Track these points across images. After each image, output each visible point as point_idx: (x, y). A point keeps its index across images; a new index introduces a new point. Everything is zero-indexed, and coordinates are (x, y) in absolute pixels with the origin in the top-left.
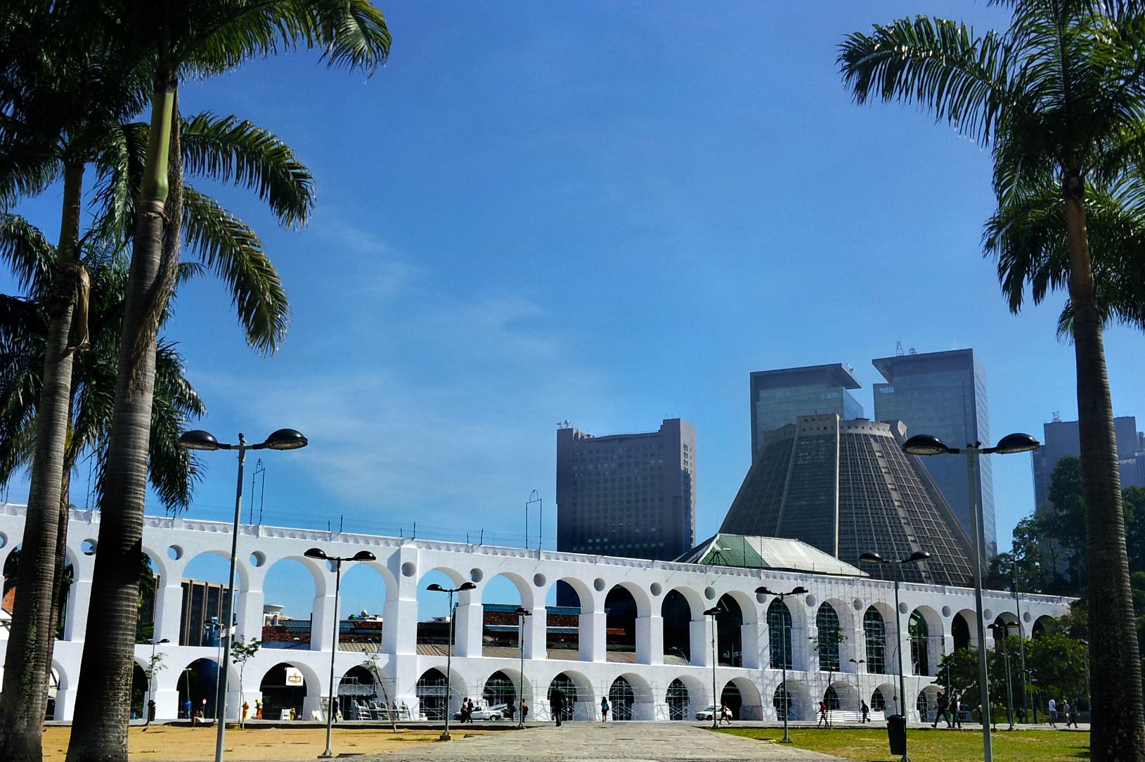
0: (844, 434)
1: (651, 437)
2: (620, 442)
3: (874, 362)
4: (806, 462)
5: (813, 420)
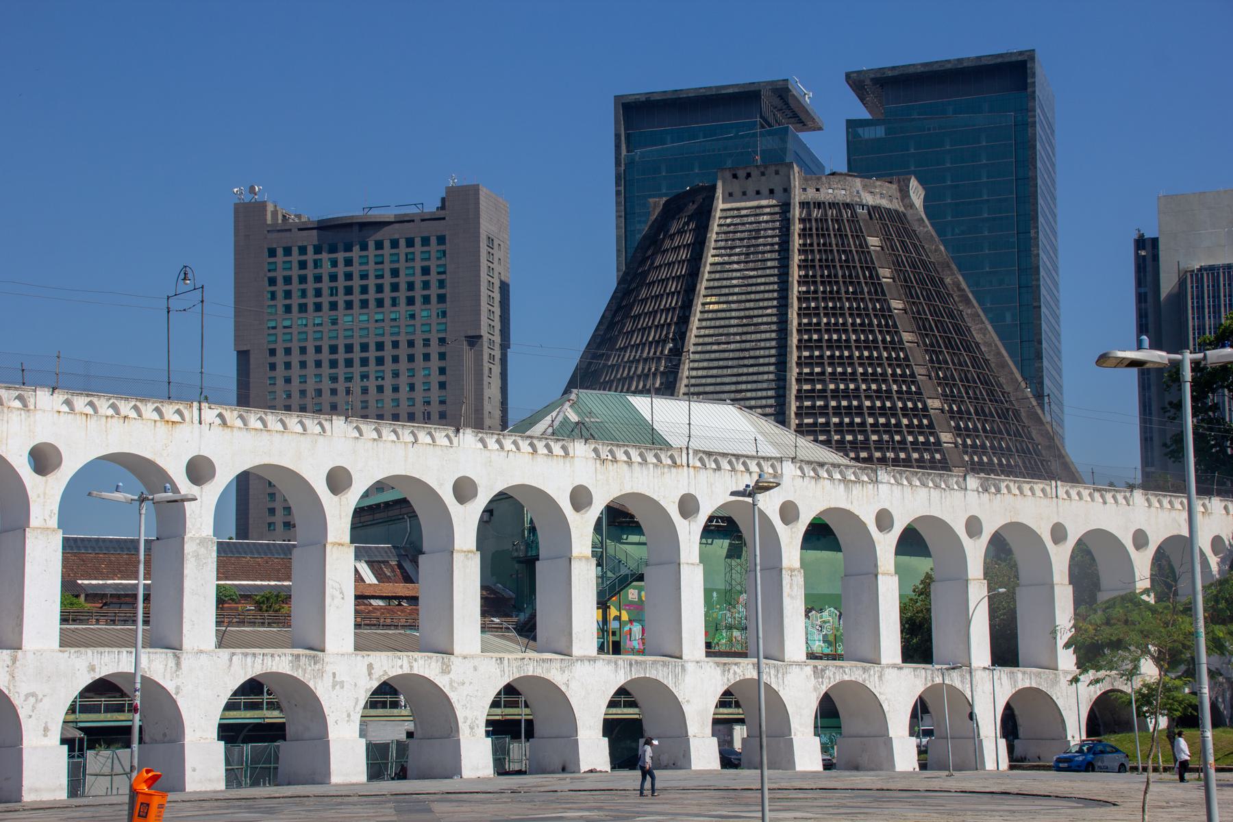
0: (808, 203)
1: (423, 220)
2: (360, 231)
3: (848, 76)
4: (735, 258)
5: (749, 175)
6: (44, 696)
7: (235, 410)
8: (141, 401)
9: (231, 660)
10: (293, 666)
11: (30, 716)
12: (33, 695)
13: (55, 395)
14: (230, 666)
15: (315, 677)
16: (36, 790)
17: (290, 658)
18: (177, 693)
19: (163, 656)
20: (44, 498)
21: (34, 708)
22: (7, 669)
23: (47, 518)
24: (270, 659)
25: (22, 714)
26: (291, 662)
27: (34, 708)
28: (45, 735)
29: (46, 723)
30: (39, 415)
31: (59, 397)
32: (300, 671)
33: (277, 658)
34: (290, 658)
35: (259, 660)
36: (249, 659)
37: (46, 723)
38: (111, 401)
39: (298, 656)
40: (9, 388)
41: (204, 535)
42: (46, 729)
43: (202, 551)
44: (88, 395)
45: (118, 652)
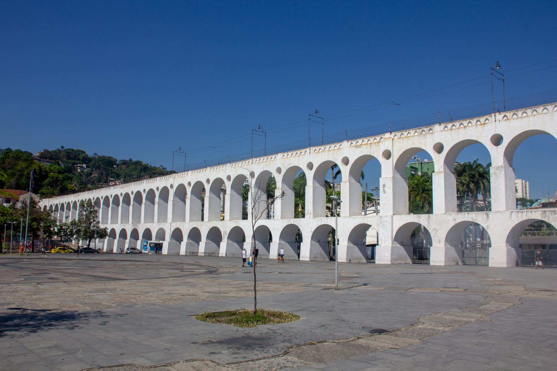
6: (439, 230)
7: (511, 112)
8: (471, 119)
9: (511, 214)
10: (542, 216)
11: (435, 237)
12: (435, 229)
13: (441, 125)
14: (511, 217)
15: (554, 220)
16: (434, 262)
17: (541, 213)
18: (488, 228)
19: (482, 214)
20: (439, 161)
21: (435, 234)
22: (427, 221)
23: (440, 168)
24: (530, 213)
25: (432, 235)
26: (541, 214)
27: (435, 234)
28: (439, 243)
29: (439, 239)
30: (436, 134)
31: (443, 126)
32: (546, 218)
33: (534, 213)
34: (541, 213)
35: (524, 214)
36: (520, 214)
37: (439, 239)
38: (460, 122)
39: (545, 211)
40: (426, 127)
41: (499, 165)
42: (440, 241)
43: (498, 171)
44: (452, 123)
45: (464, 213)
